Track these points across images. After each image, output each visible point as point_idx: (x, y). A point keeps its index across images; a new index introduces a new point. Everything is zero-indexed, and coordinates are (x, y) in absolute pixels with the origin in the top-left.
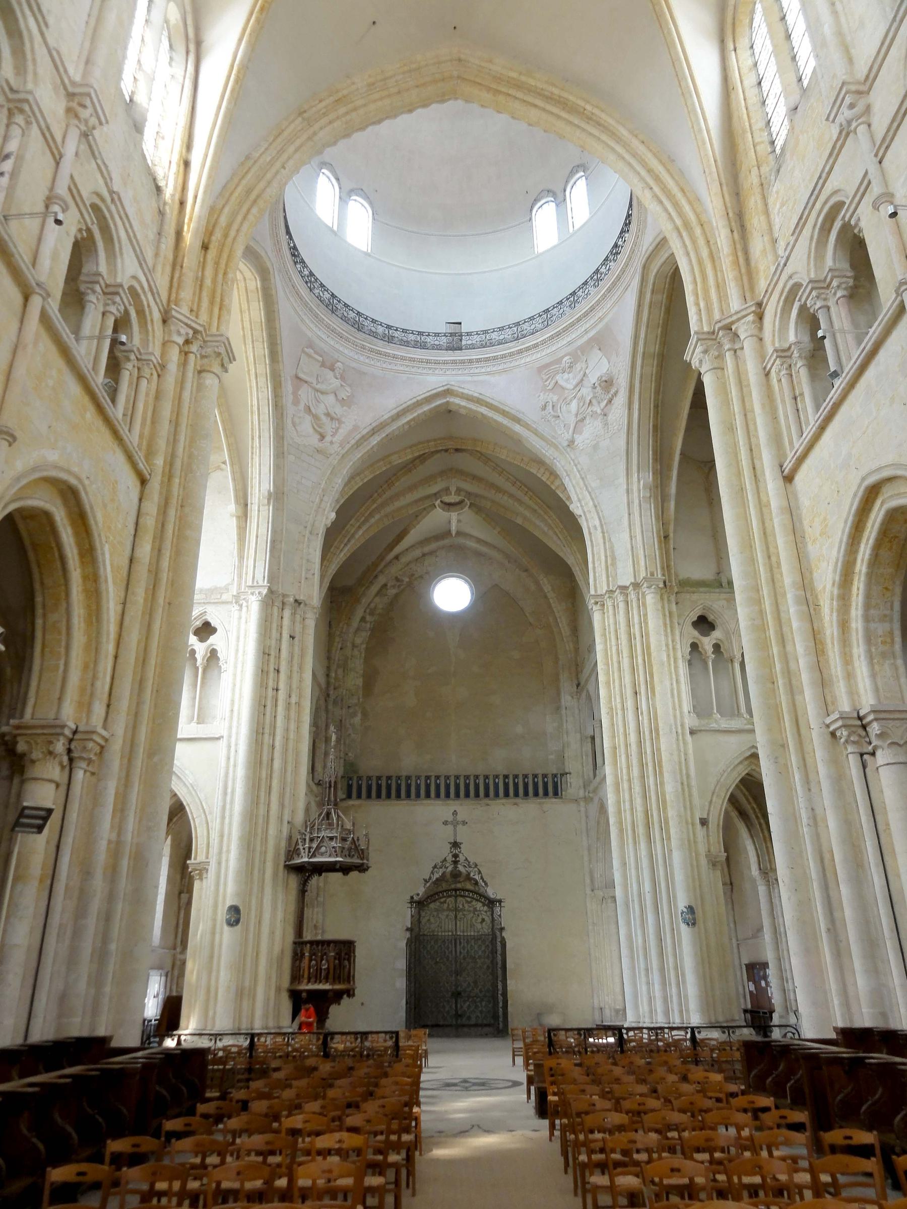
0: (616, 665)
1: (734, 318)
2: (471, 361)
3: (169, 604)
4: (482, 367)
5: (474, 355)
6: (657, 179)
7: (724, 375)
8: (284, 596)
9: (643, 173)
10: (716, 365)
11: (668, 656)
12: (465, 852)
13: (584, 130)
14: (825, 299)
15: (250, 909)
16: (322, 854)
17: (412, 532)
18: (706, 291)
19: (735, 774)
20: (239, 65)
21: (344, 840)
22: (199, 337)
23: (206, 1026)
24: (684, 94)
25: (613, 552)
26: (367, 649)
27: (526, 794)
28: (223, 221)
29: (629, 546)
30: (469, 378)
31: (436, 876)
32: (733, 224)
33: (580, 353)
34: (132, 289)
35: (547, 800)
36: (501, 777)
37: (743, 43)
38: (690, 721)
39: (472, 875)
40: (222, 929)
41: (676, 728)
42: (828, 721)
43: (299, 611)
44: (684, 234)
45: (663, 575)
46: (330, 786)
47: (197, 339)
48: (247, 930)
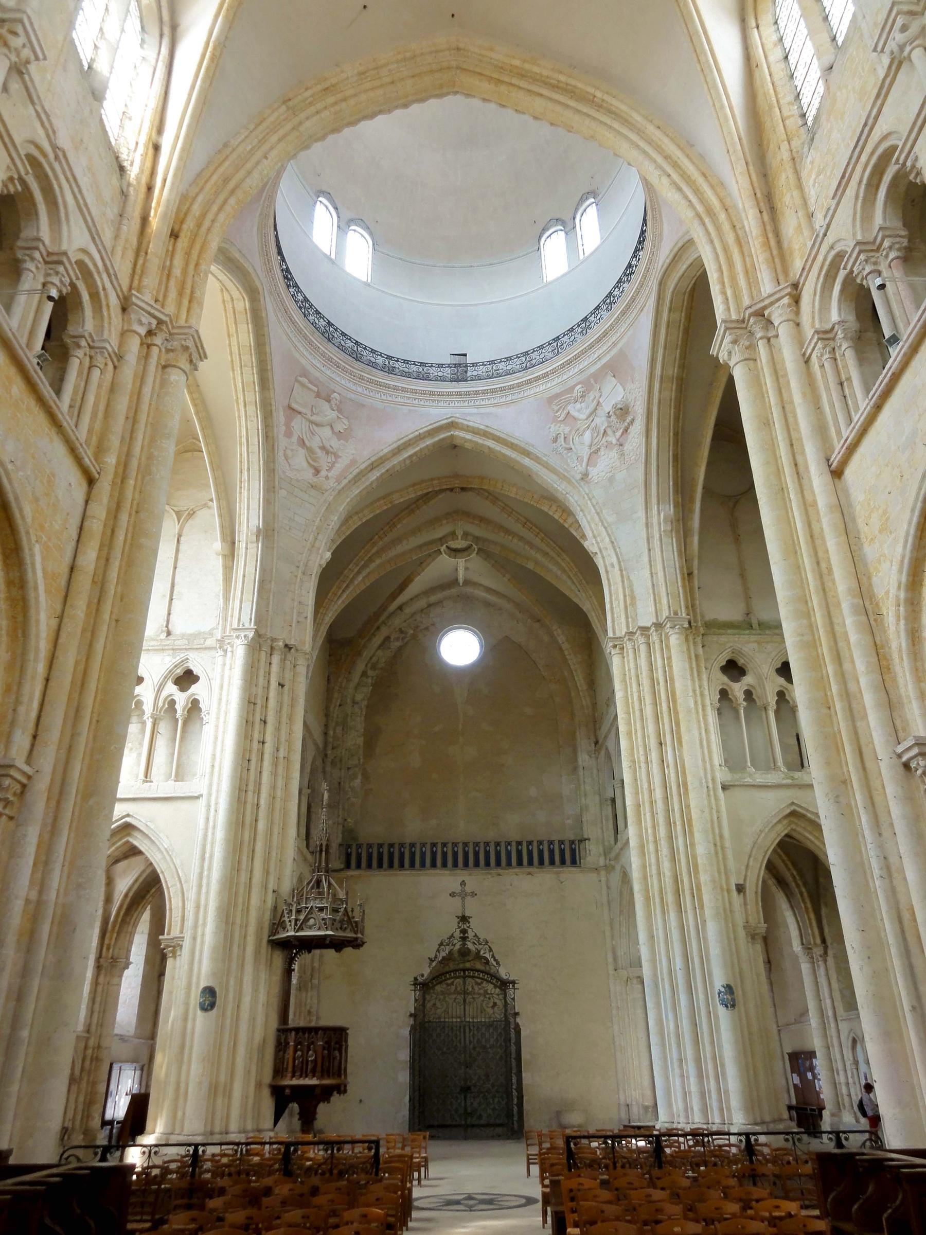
0: (638, 713)
1: (767, 302)
3: (117, 621)
4: (489, 399)
5: (480, 386)
6: (676, 165)
8: (273, 640)
9: (660, 160)
10: (747, 356)
11: (696, 702)
12: (476, 927)
13: (594, 118)
14: (875, 263)
15: (227, 990)
16: (310, 927)
17: (417, 579)
18: (733, 278)
19: (773, 835)
20: (215, 42)
21: (335, 911)
22: (164, 328)
23: (174, 1129)
24: (704, 70)
25: (632, 591)
26: (368, 706)
27: (541, 863)
28: (196, 209)
29: (650, 584)
30: (475, 411)
31: (443, 954)
32: (762, 204)
33: (592, 382)
34: (80, 264)
35: (565, 869)
36: (514, 844)
37: (766, 20)
38: (722, 775)
39: (482, 953)
40: (195, 1015)
41: (707, 782)
42: (900, 749)
43: (289, 657)
44: (707, 220)
45: (688, 615)
46: (321, 851)
47: (161, 330)
48: (224, 1014)
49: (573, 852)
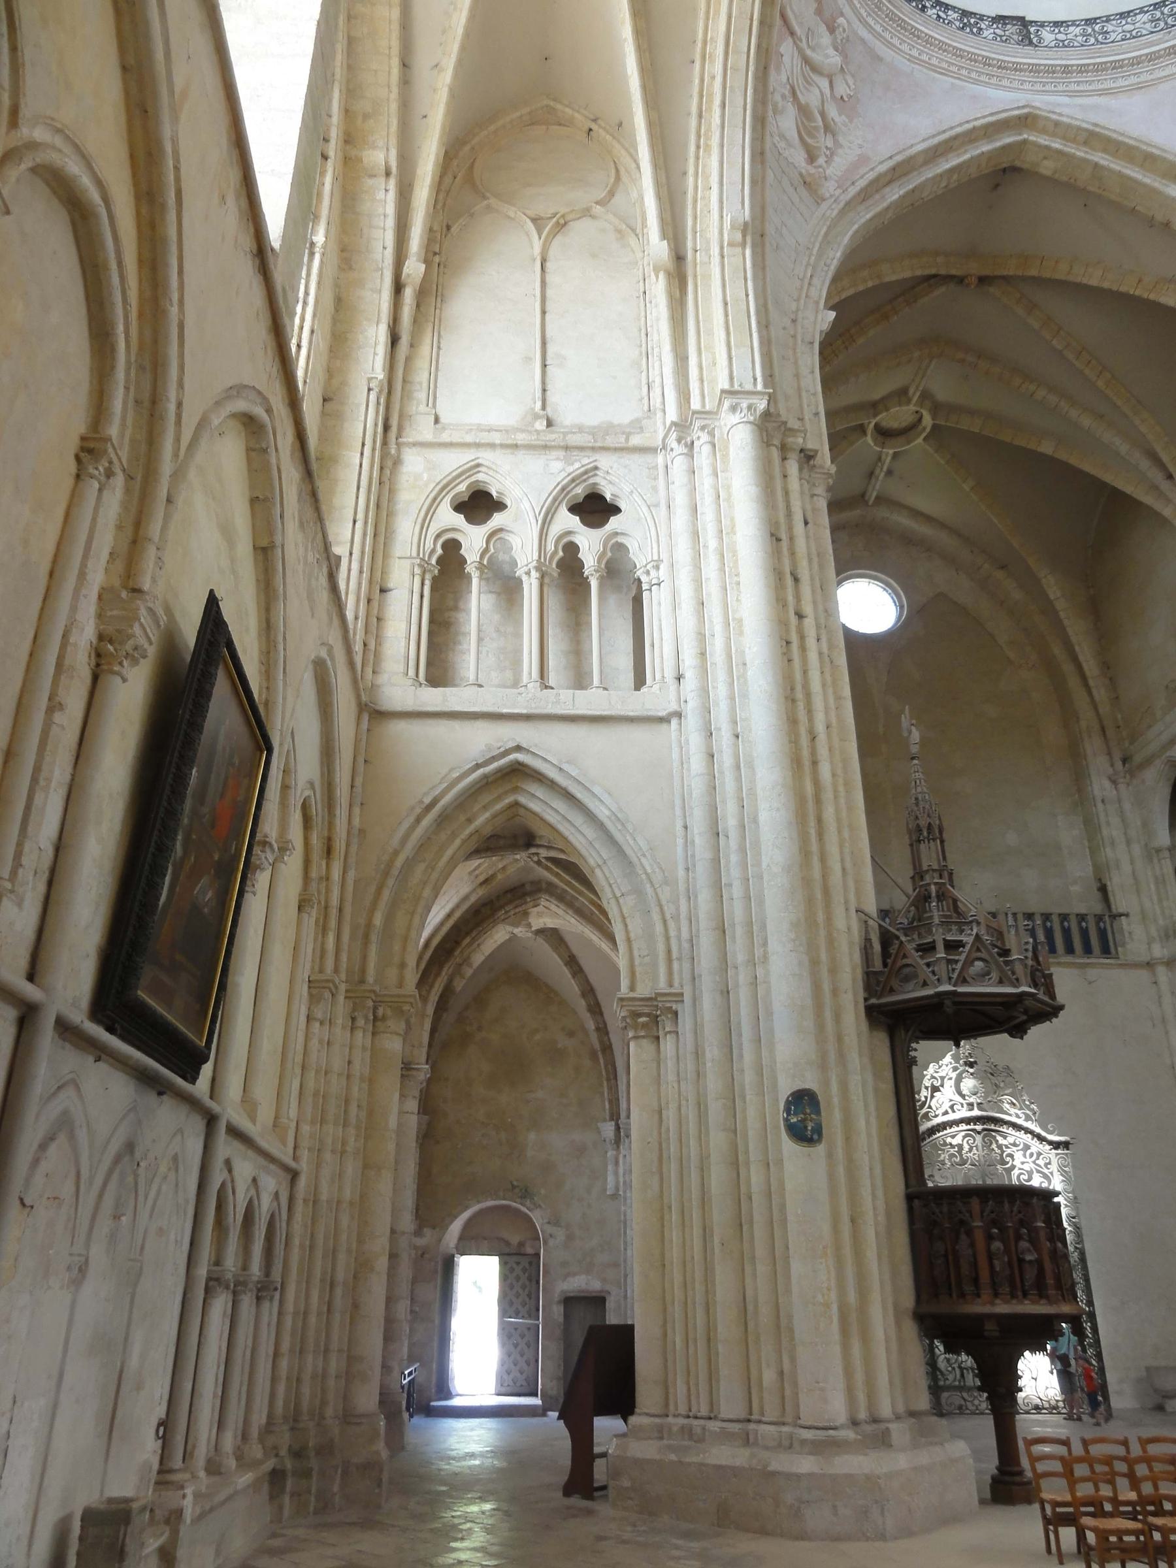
2: (1067, 69)
4: (1091, 83)
30: (1066, 100)
49: (1103, 935)
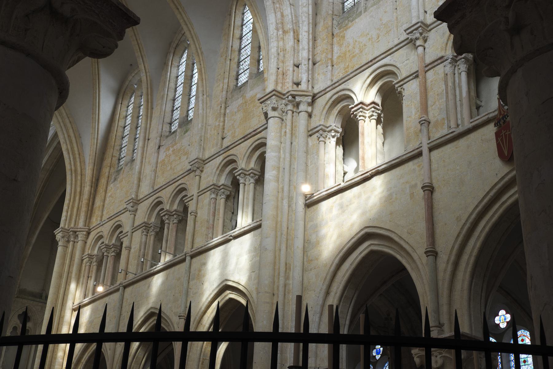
1: (78, 230)
6: (71, 142)
7: (66, 250)
9: (66, 136)
10: (65, 245)
37: (125, 103)
